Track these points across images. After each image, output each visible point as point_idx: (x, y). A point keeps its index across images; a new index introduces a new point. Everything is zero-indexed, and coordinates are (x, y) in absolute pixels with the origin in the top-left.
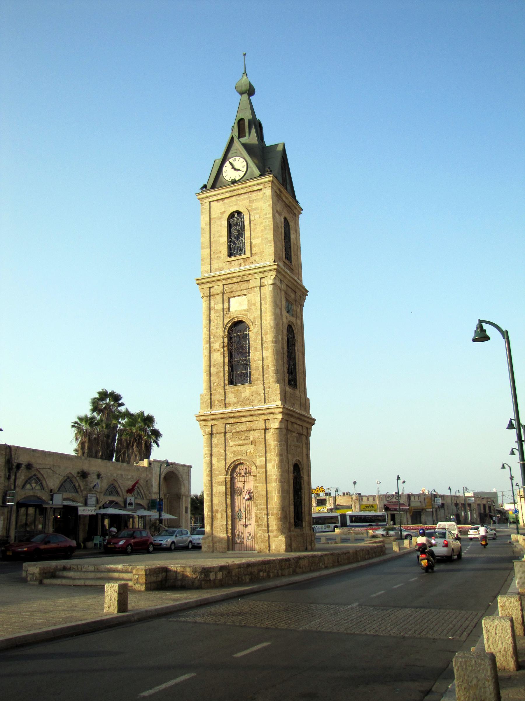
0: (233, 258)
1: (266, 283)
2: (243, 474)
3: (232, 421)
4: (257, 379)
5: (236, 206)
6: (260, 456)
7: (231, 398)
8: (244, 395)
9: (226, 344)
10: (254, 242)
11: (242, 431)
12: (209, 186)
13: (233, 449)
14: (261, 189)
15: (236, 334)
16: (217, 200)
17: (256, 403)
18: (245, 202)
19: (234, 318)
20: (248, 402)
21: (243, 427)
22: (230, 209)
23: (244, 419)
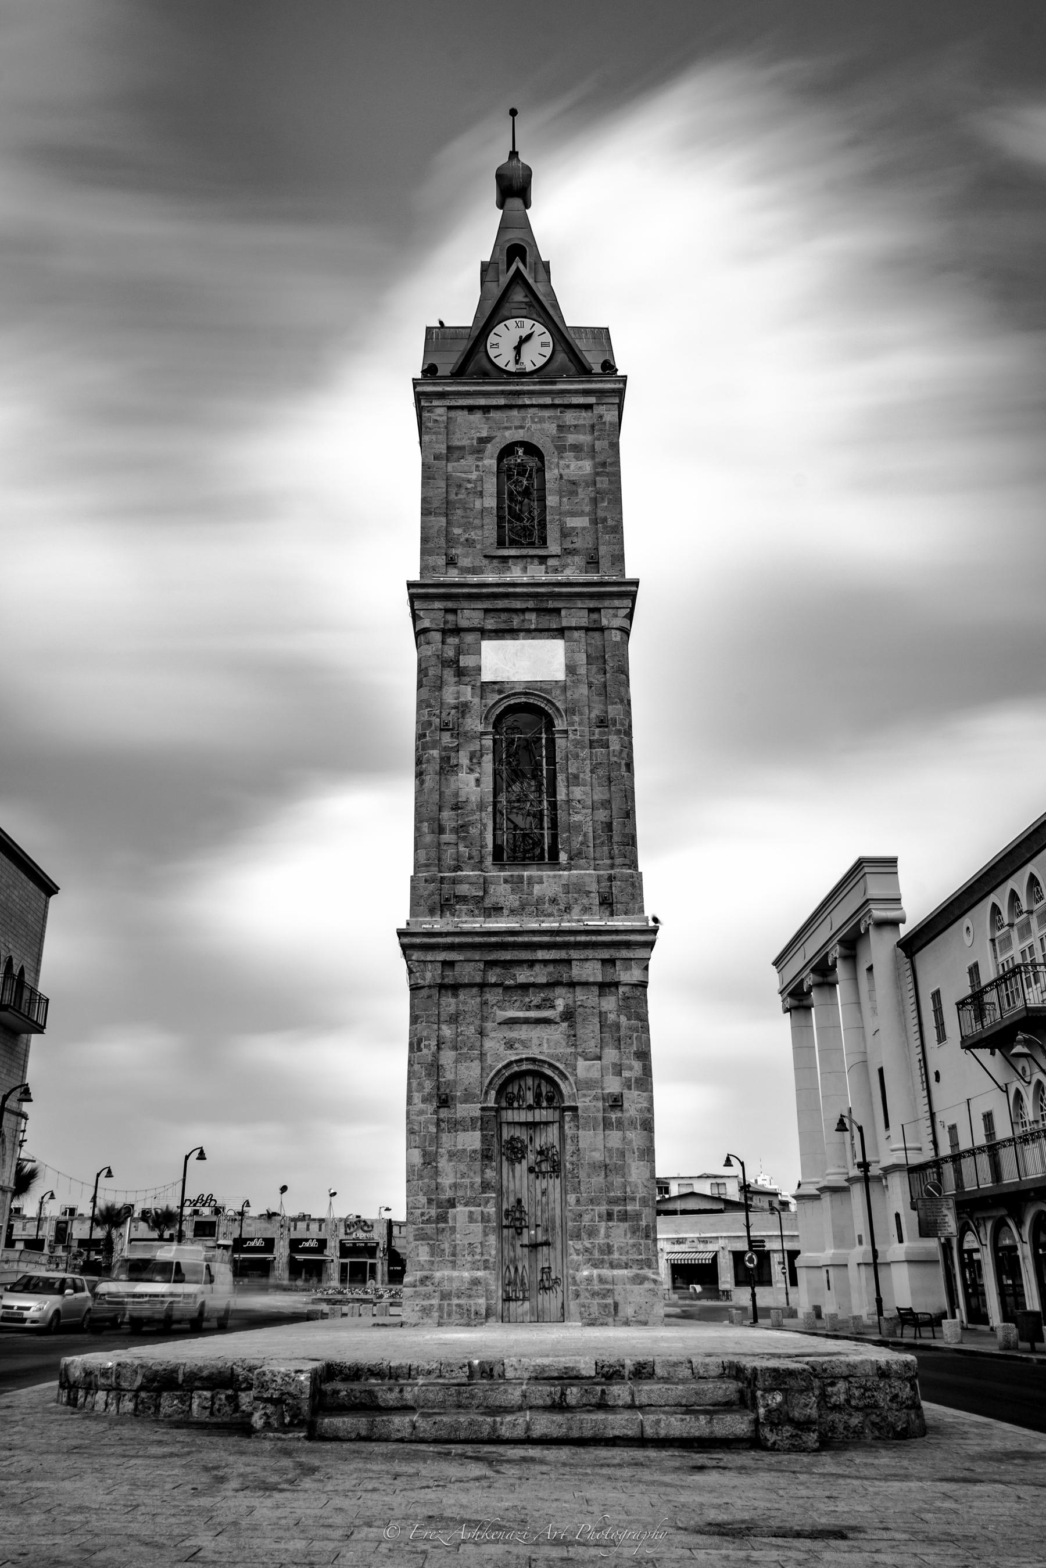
0: (513, 552)
1: (605, 622)
2: (530, 1099)
5: (521, 431)
7: (501, 893)
10: (572, 522)
11: (534, 985)
12: (444, 370)
14: (588, 407)
16: (471, 409)
18: (546, 426)
19: (515, 694)
22: (507, 433)
23: (541, 955)
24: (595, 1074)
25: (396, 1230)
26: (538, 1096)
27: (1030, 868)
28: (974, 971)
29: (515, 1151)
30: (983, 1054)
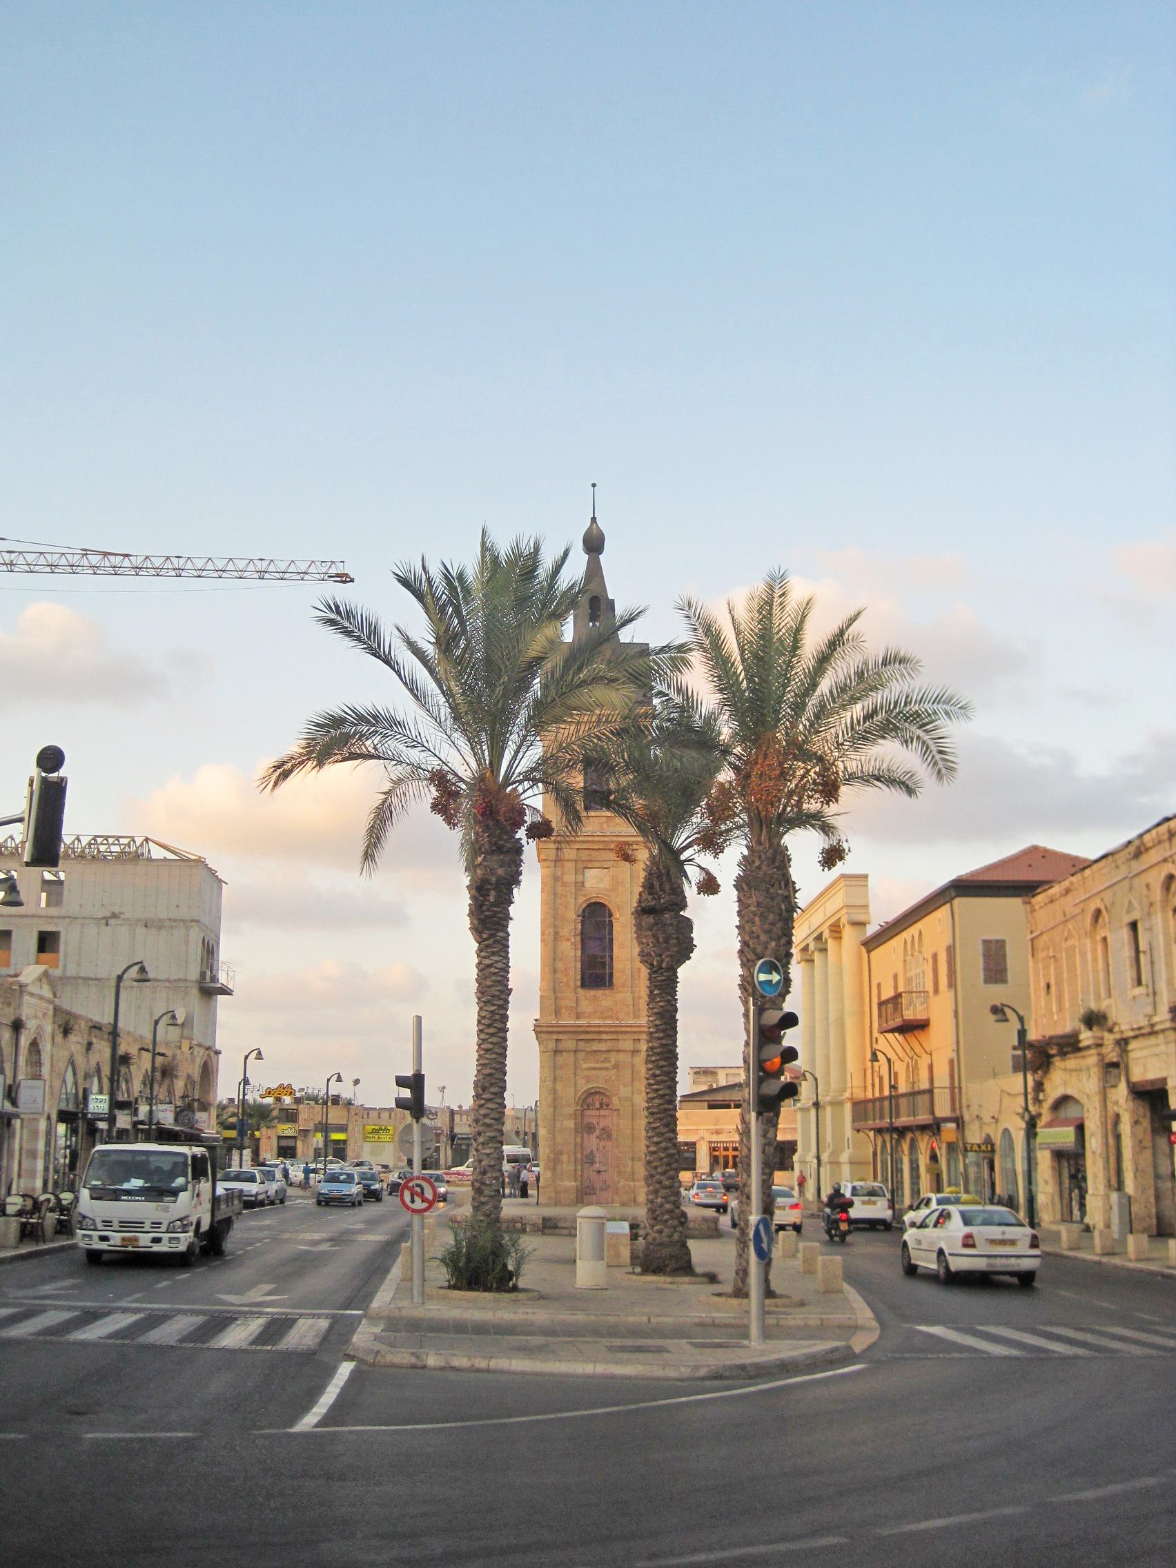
2: (598, 1105)
3: (588, 1037)
4: (623, 986)
6: (625, 1086)
7: (585, 1006)
8: (604, 1003)
9: (579, 931)
13: (586, 1073)
15: (596, 918)
17: (621, 1015)
20: (610, 1014)
21: (603, 1047)
23: (604, 1037)
24: (628, 1094)
25: (457, 1118)
26: (601, 1104)
27: (919, 926)
28: (895, 977)
29: (590, 1129)
30: (889, 1036)
